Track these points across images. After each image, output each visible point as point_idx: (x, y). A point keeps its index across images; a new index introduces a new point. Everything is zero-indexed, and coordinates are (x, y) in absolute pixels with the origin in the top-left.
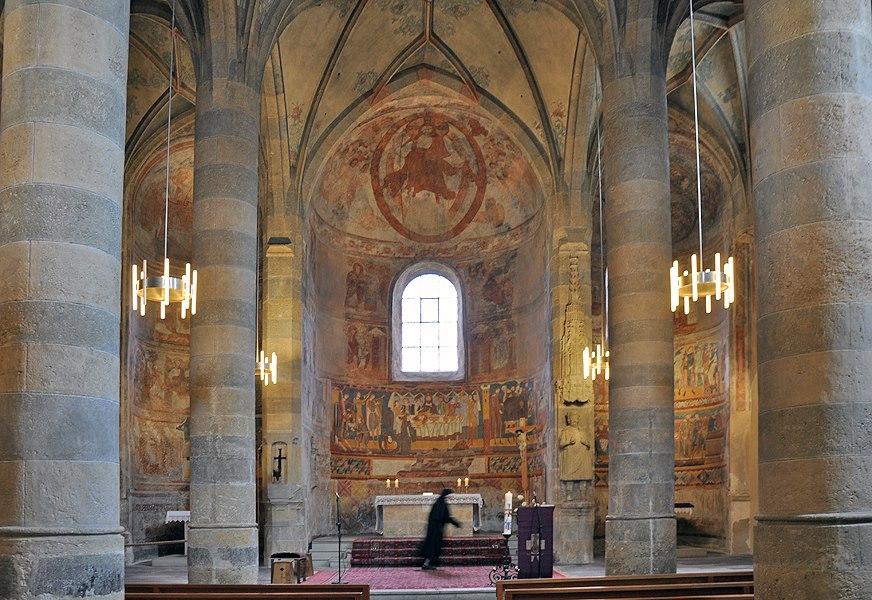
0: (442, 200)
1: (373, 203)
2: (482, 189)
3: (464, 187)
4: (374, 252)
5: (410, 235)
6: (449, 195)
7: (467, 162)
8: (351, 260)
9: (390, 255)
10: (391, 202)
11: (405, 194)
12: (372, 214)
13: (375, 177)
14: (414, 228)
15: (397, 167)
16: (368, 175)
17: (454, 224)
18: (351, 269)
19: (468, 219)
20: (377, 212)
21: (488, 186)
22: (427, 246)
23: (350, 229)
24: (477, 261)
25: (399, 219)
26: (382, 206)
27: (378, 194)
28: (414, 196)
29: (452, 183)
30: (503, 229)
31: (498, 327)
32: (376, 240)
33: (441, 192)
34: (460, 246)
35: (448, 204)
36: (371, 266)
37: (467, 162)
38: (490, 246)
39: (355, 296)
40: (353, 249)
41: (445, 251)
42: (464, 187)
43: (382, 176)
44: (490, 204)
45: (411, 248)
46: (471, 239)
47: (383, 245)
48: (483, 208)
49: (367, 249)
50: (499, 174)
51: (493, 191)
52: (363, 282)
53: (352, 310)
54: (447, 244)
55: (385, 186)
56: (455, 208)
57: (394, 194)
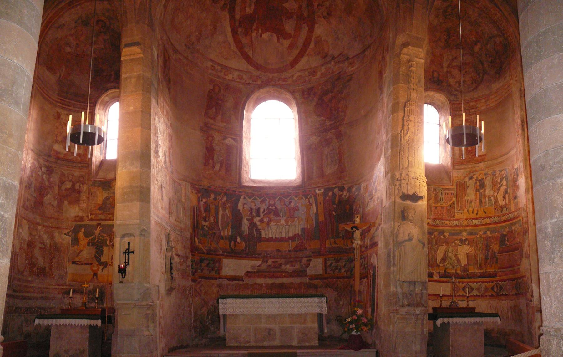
0: (282, 40)
1: (230, 39)
2: (311, 30)
3: (298, 29)
4: (230, 77)
5: (258, 67)
6: (286, 36)
7: (301, 7)
8: (211, 81)
9: (243, 81)
10: (244, 40)
11: (254, 35)
12: (230, 48)
13: (232, 18)
14: (261, 61)
15: (249, 11)
16: (226, 13)
17: (291, 59)
18: (211, 87)
19: (301, 54)
20: (234, 48)
21: (316, 26)
22: (270, 75)
23: (212, 56)
24: (309, 86)
25: (250, 54)
26: (238, 42)
27: (234, 32)
28: (261, 36)
29: (289, 26)
30: (328, 59)
31: (328, 137)
32: (232, 68)
33: (282, 34)
34: (295, 76)
35: (286, 43)
36: (227, 87)
37: (301, 7)
38: (318, 74)
39: (214, 109)
40: (214, 72)
41: (285, 80)
42: (298, 29)
43: (238, 17)
44: (319, 41)
45: (258, 77)
46: (305, 70)
47: (236, 73)
48: (312, 45)
49: (225, 75)
50: (325, 14)
51: (319, 30)
52: (221, 100)
53: (211, 121)
54: (286, 74)
55: (240, 26)
56: (291, 47)
57: (246, 34)
